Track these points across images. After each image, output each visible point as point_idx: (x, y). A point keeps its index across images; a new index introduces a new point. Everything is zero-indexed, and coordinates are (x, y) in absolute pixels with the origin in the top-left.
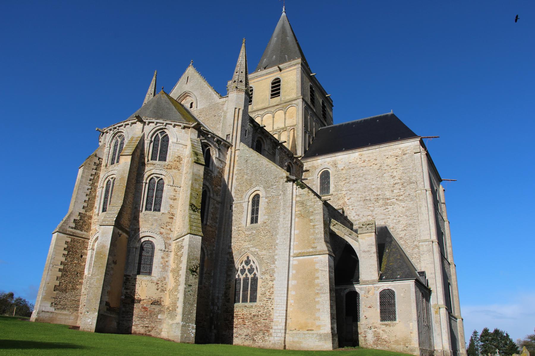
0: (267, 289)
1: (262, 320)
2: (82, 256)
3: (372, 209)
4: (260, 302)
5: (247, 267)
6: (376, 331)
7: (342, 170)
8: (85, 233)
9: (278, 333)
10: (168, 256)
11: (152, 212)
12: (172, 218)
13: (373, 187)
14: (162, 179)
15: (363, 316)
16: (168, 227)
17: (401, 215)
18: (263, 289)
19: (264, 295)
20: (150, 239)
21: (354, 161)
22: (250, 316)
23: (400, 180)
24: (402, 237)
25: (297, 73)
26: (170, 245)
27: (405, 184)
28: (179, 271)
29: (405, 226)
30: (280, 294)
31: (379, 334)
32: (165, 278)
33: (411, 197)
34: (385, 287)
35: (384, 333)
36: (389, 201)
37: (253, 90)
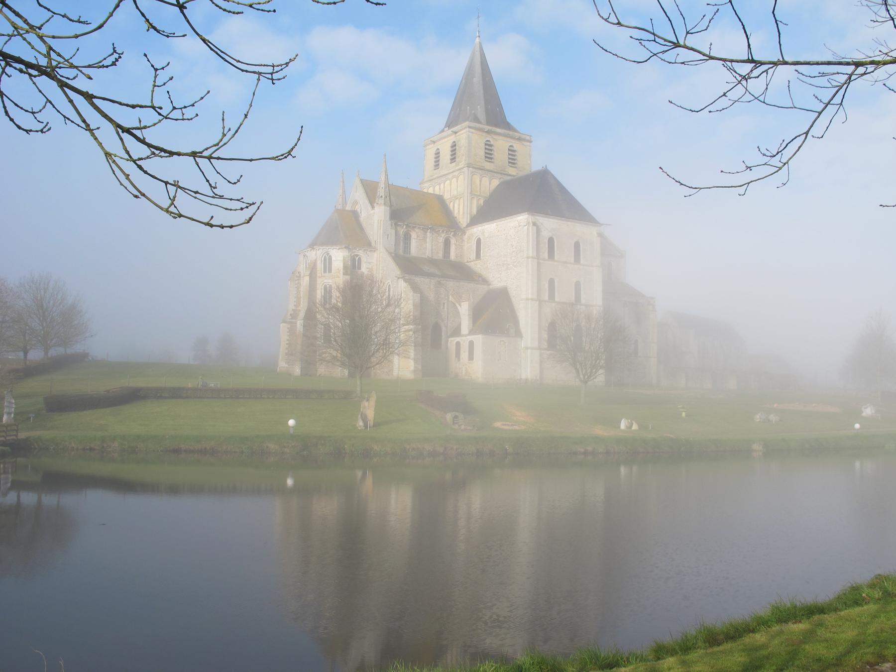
7: (487, 238)
14: (330, 285)
36: (509, 266)
37: (439, 152)
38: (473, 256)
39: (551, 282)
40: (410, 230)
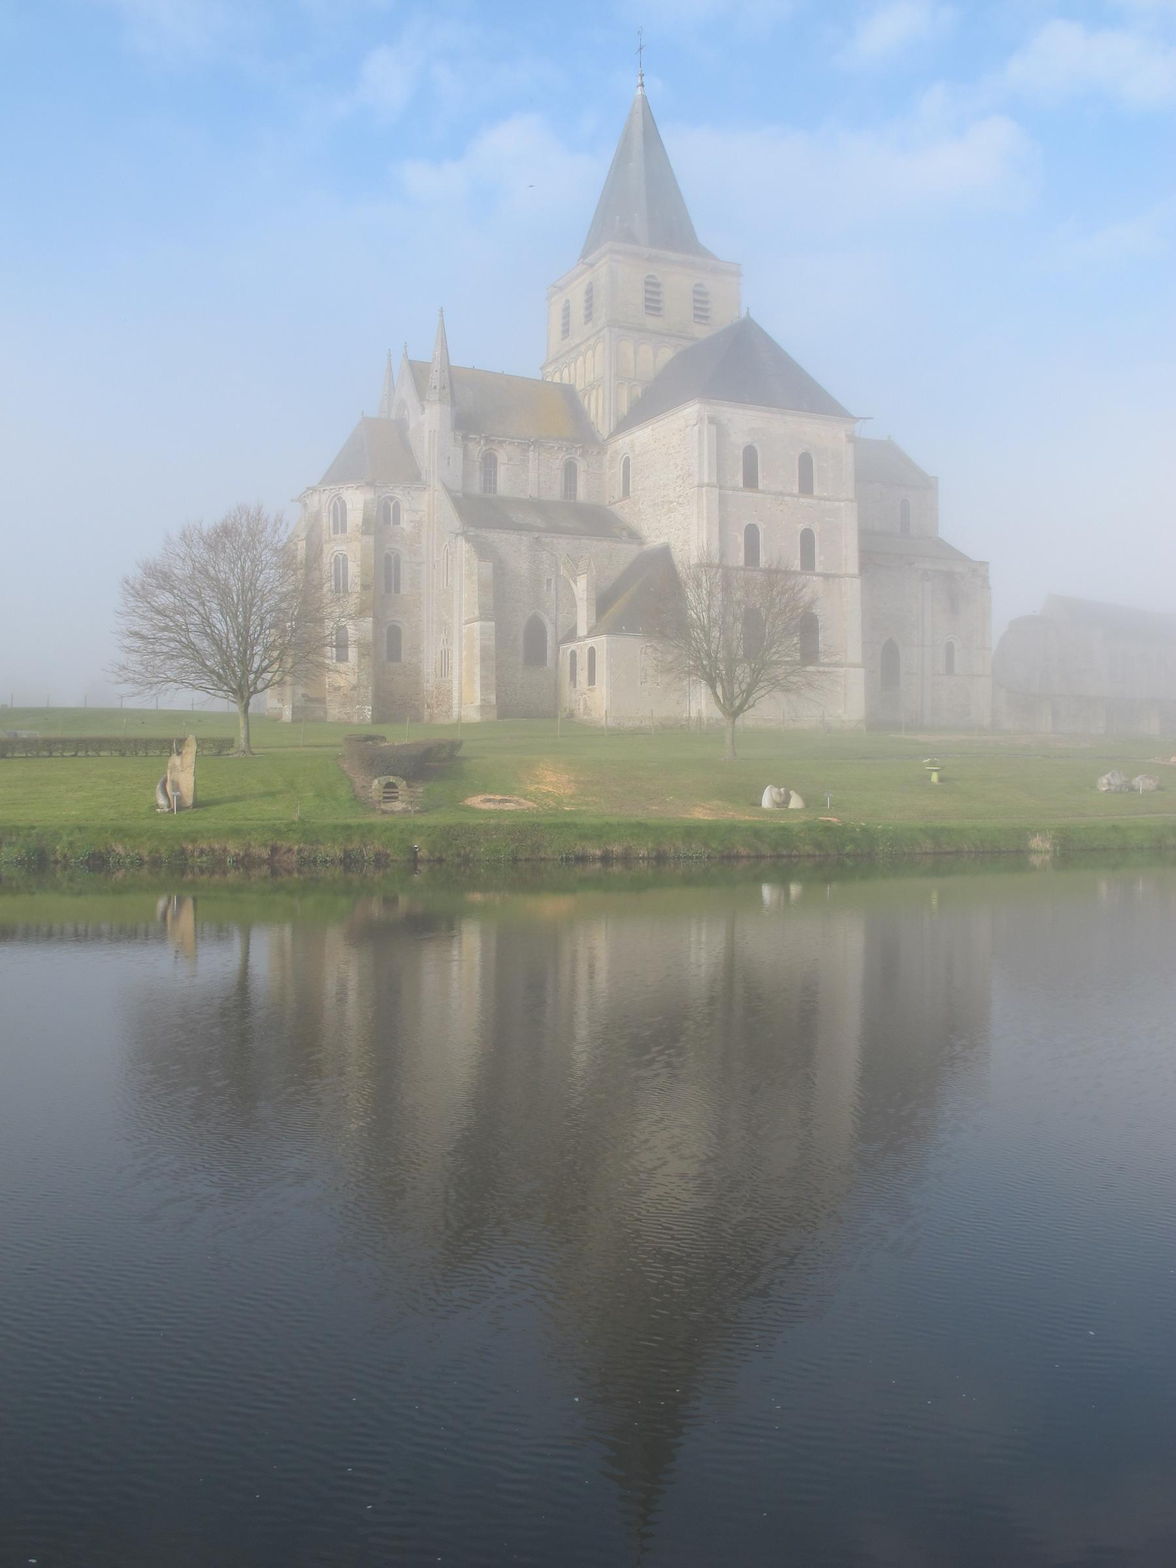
14: (345, 555)
36: (671, 506)
38: (618, 492)
39: (752, 534)
40: (494, 447)
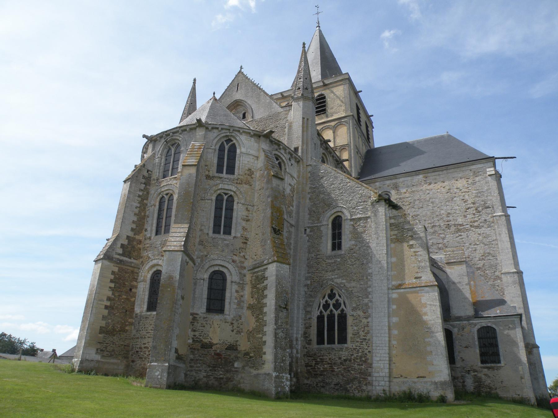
0: (360, 328)
1: (356, 366)
2: (131, 290)
3: (442, 236)
4: (352, 344)
5: (331, 302)
6: (476, 375)
8: (135, 261)
9: (380, 382)
10: (243, 289)
11: (222, 236)
12: (246, 243)
13: (442, 212)
14: (231, 196)
15: (459, 358)
16: (242, 254)
17: (478, 243)
18: (355, 328)
19: (356, 335)
20: (221, 269)
21: (417, 183)
22: (339, 361)
23: (474, 204)
24: (480, 268)
25: (344, 88)
26: (245, 276)
27: (480, 209)
28: (261, 307)
29: (483, 255)
30: (379, 333)
31: (480, 378)
32: (240, 317)
33: (488, 223)
34: (483, 324)
35: (486, 377)
